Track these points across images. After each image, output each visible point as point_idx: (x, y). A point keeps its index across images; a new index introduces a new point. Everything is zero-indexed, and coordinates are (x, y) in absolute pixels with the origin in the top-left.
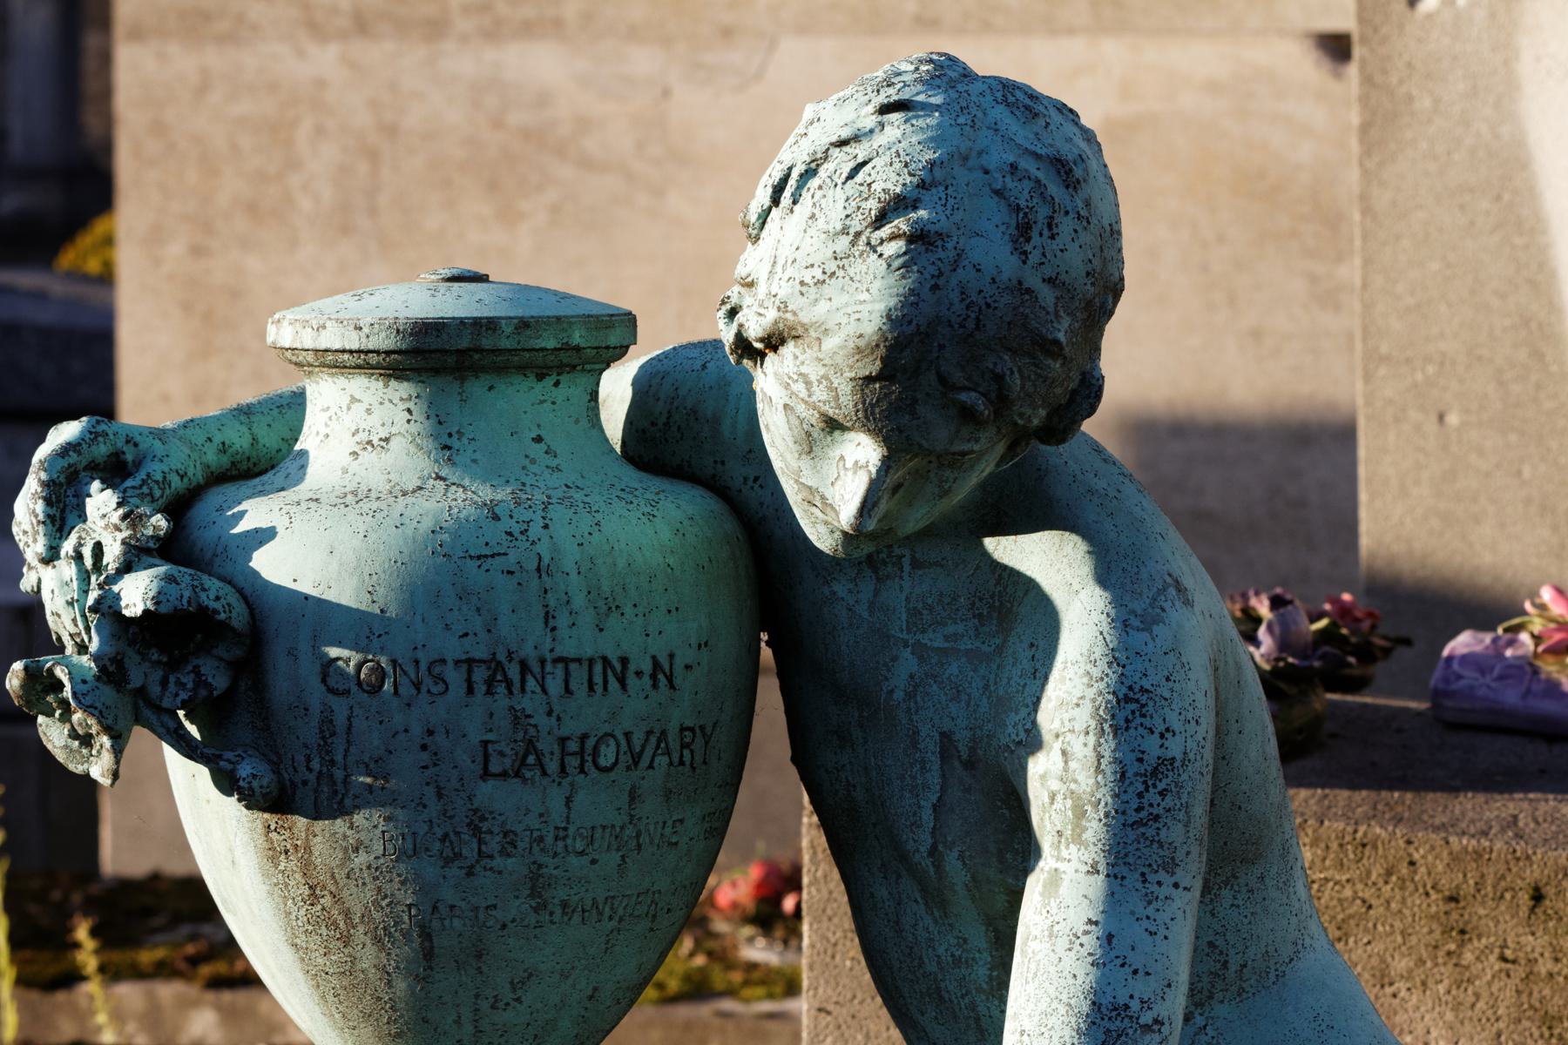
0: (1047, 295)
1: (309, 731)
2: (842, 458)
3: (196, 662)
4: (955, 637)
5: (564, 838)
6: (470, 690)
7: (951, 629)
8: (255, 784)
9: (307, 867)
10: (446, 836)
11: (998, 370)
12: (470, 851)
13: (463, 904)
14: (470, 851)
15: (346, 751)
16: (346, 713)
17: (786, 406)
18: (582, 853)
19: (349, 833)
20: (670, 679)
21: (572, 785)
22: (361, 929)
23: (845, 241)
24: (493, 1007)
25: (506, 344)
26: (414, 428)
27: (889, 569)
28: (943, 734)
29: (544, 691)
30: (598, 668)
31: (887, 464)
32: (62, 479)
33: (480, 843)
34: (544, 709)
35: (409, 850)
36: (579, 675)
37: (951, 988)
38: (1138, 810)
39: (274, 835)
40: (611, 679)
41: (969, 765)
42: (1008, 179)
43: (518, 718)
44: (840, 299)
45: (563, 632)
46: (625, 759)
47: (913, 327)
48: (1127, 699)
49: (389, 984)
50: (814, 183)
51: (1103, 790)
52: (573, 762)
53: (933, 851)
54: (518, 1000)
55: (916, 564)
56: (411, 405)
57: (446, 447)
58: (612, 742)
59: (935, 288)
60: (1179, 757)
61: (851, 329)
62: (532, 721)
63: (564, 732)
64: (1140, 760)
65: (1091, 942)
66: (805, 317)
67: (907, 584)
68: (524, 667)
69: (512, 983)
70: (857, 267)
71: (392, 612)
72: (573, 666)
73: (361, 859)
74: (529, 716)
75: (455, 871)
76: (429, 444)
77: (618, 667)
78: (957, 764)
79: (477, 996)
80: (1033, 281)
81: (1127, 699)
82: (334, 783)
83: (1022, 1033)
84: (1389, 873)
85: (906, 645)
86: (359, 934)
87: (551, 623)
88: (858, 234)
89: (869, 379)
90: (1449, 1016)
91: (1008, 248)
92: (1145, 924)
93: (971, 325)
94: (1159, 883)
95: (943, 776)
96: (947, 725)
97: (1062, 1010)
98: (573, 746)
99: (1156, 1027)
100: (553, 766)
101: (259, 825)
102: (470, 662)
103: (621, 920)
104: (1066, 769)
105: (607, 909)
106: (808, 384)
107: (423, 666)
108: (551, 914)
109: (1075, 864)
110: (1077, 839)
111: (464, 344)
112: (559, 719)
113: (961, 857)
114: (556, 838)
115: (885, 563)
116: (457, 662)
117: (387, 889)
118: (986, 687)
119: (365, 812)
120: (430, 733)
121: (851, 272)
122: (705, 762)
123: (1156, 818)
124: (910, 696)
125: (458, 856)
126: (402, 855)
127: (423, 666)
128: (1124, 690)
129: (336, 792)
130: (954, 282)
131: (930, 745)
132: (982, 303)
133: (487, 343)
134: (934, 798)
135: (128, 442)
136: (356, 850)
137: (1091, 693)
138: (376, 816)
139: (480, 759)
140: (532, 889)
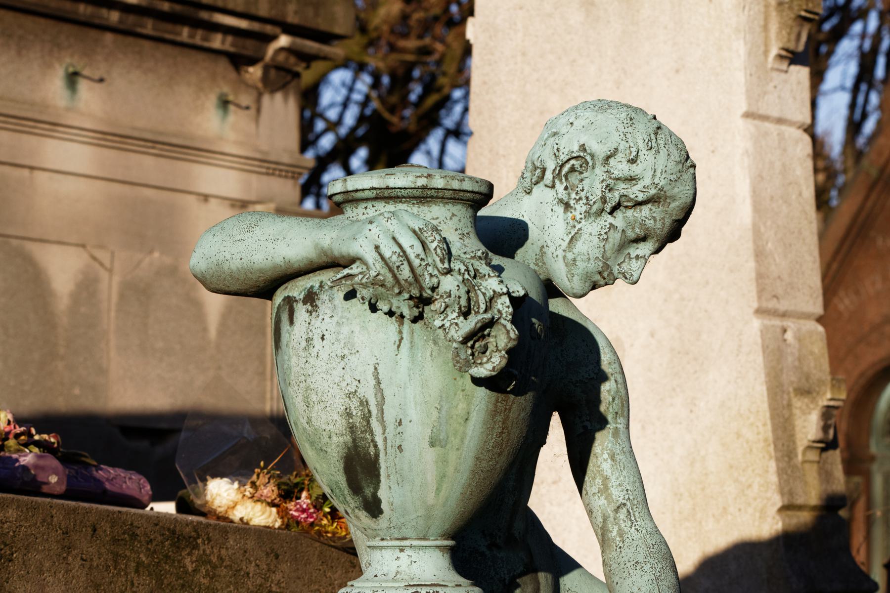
2: (629, 254)
17: (623, 231)
23: (680, 166)
44: (682, 188)
61: (683, 200)
66: (668, 194)
83: (627, 490)
84: (44, 521)
90: (63, 588)
101: (493, 399)
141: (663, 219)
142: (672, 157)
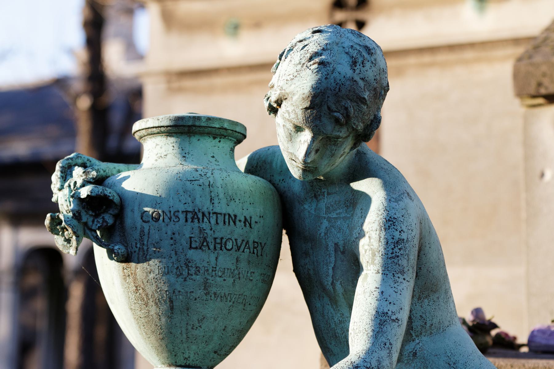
0: (361, 83)
1: (137, 235)
2: (300, 141)
3: (103, 215)
4: (340, 213)
5: (215, 271)
6: (186, 221)
7: (338, 211)
8: (119, 251)
9: (135, 279)
10: (178, 267)
11: (346, 106)
12: (185, 273)
13: (183, 291)
14: (185, 273)
15: (148, 240)
16: (148, 228)
17: (283, 125)
18: (221, 277)
19: (148, 267)
20: (250, 225)
21: (218, 253)
22: (151, 300)
24: (192, 328)
25: (203, 124)
26: (175, 151)
27: (321, 197)
28: (335, 244)
29: (210, 222)
30: (227, 217)
31: (314, 139)
32: (66, 166)
33: (188, 270)
34: (209, 228)
35: (166, 272)
36: (221, 218)
37: (339, 332)
38: (392, 253)
39: (125, 271)
40: (231, 221)
41: (343, 253)
42: (350, 49)
43: (201, 230)
45: (216, 204)
46: (235, 248)
47: (319, 90)
48: (389, 220)
49: (160, 319)
50: (291, 52)
51: (381, 247)
52: (218, 246)
53: (333, 284)
54: (200, 326)
55: (328, 194)
56: (174, 145)
57: (184, 157)
58: (231, 241)
59: (326, 78)
60: (406, 239)
61: (301, 92)
62: (206, 231)
63: (216, 236)
64: (393, 238)
65: (376, 294)
66: (287, 91)
67: (325, 200)
68: (204, 215)
69: (198, 320)
70: (303, 74)
71: (163, 196)
72: (219, 215)
73: (152, 276)
74: (204, 230)
75: (180, 279)
76: (179, 156)
77: (233, 218)
78: (339, 253)
79: (187, 324)
80: (357, 78)
81: (389, 220)
82: (144, 251)
85: (325, 218)
86: (151, 303)
87: (213, 201)
88: (304, 64)
89: (306, 109)
91: (350, 68)
92: (394, 289)
93: (337, 90)
94: (399, 277)
95: (335, 258)
96: (336, 241)
97: (367, 314)
98: (218, 241)
99: (397, 321)
100: (212, 247)
101: (121, 268)
102: (187, 212)
103: (233, 303)
104: (370, 242)
105: (229, 298)
106: (289, 113)
107: (172, 213)
108: (211, 296)
109: (372, 271)
110: (373, 263)
111: (190, 124)
112: (214, 232)
113: (341, 284)
114: (213, 271)
115: (319, 195)
116: (183, 212)
117: (159, 285)
118: (348, 226)
119: (153, 260)
120: (174, 234)
121: (301, 75)
122: (261, 255)
123: (398, 256)
124: (326, 234)
125: (181, 274)
126: (165, 274)
127: (172, 213)
128: (388, 218)
129: (144, 254)
130: (332, 77)
131: (331, 248)
132: (341, 83)
133: (197, 124)
134: (333, 265)
135: (88, 160)
136: (150, 273)
137: (378, 219)
138: (156, 261)
139: (189, 243)
140: (205, 287)
141: (294, 110)
142: (293, 62)
